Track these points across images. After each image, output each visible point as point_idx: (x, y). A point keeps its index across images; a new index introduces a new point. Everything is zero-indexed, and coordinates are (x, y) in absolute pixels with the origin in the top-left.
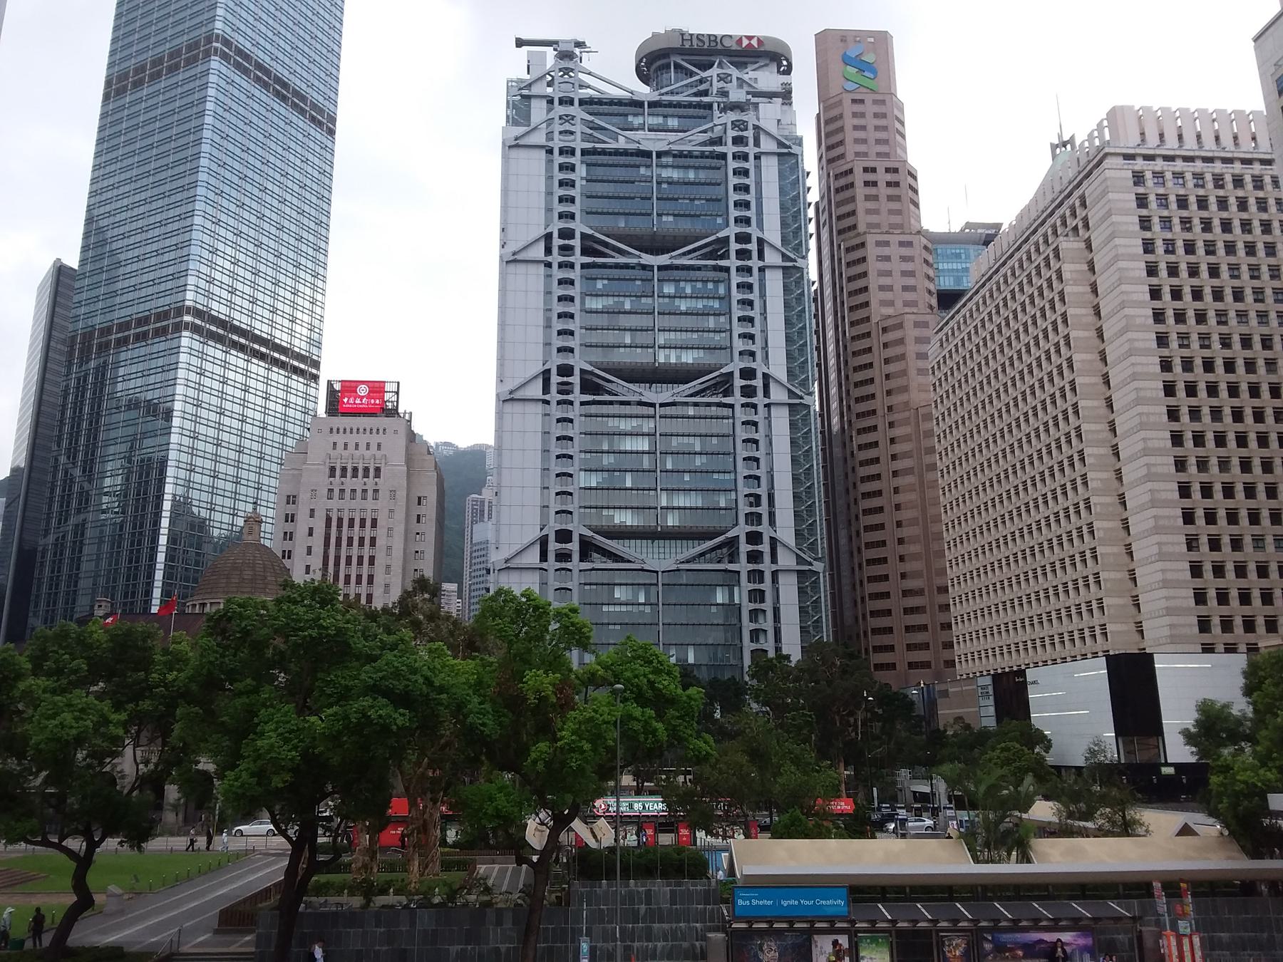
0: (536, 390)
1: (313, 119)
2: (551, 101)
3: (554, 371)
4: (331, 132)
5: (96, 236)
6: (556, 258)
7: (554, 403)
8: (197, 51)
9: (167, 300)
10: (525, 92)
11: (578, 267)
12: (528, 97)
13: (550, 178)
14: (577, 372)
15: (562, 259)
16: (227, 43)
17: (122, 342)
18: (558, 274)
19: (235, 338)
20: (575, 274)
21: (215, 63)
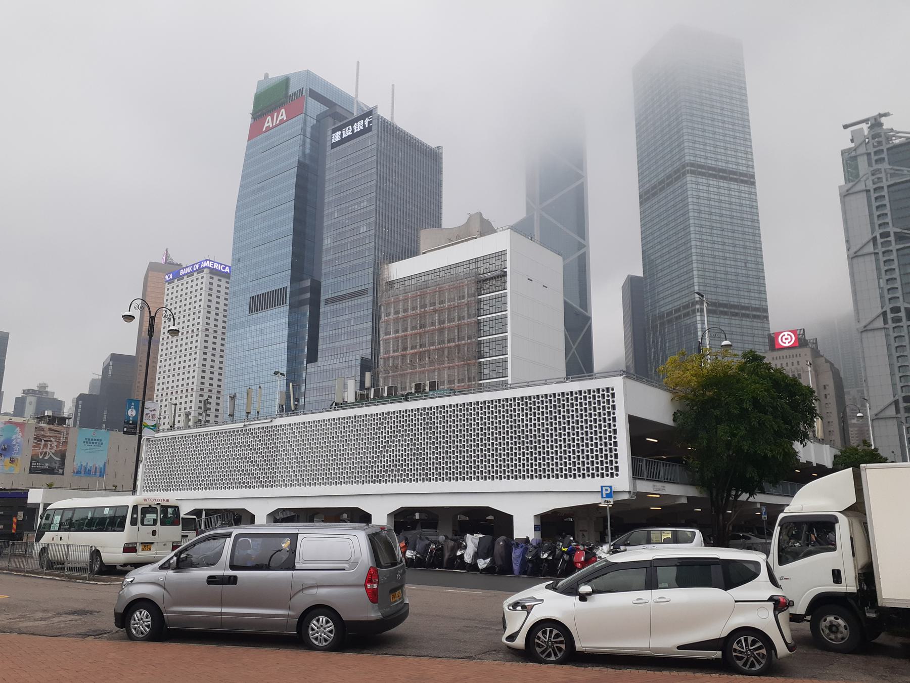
0: (880, 323)
1: (742, 182)
2: (869, 154)
3: (889, 312)
4: (753, 183)
5: (648, 262)
6: (880, 250)
7: (891, 330)
8: (678, 174)
9: (687, 299)
10: (853, 154)
11: (895, 252)
12: (855, 158)
13: (870, 205)
14: (903, 310)
15: (884, 249)
16: (692, 165)
17: (670, 321)
18: (882, 259)
19: (721, 309)
20: (894, 256)
21: (689, 178)
